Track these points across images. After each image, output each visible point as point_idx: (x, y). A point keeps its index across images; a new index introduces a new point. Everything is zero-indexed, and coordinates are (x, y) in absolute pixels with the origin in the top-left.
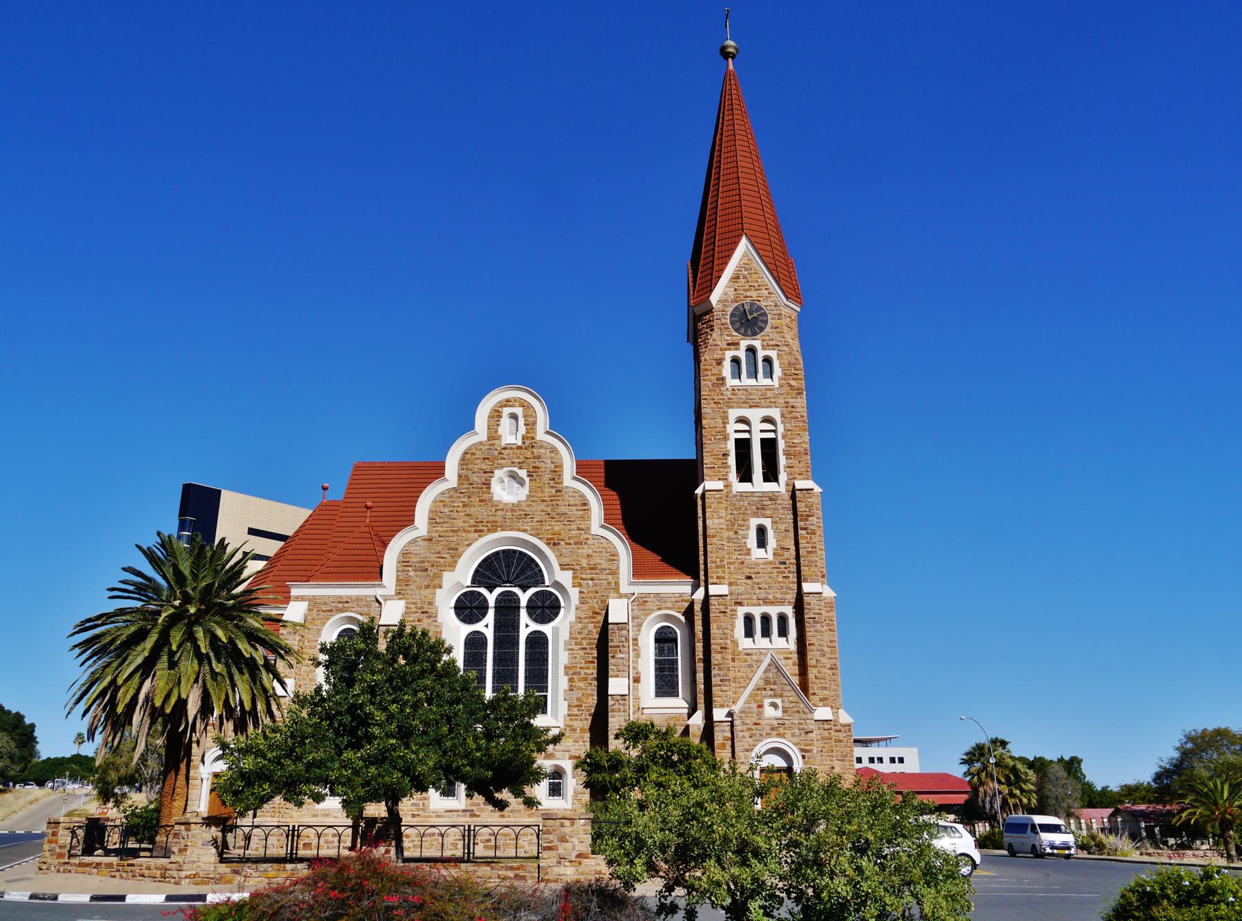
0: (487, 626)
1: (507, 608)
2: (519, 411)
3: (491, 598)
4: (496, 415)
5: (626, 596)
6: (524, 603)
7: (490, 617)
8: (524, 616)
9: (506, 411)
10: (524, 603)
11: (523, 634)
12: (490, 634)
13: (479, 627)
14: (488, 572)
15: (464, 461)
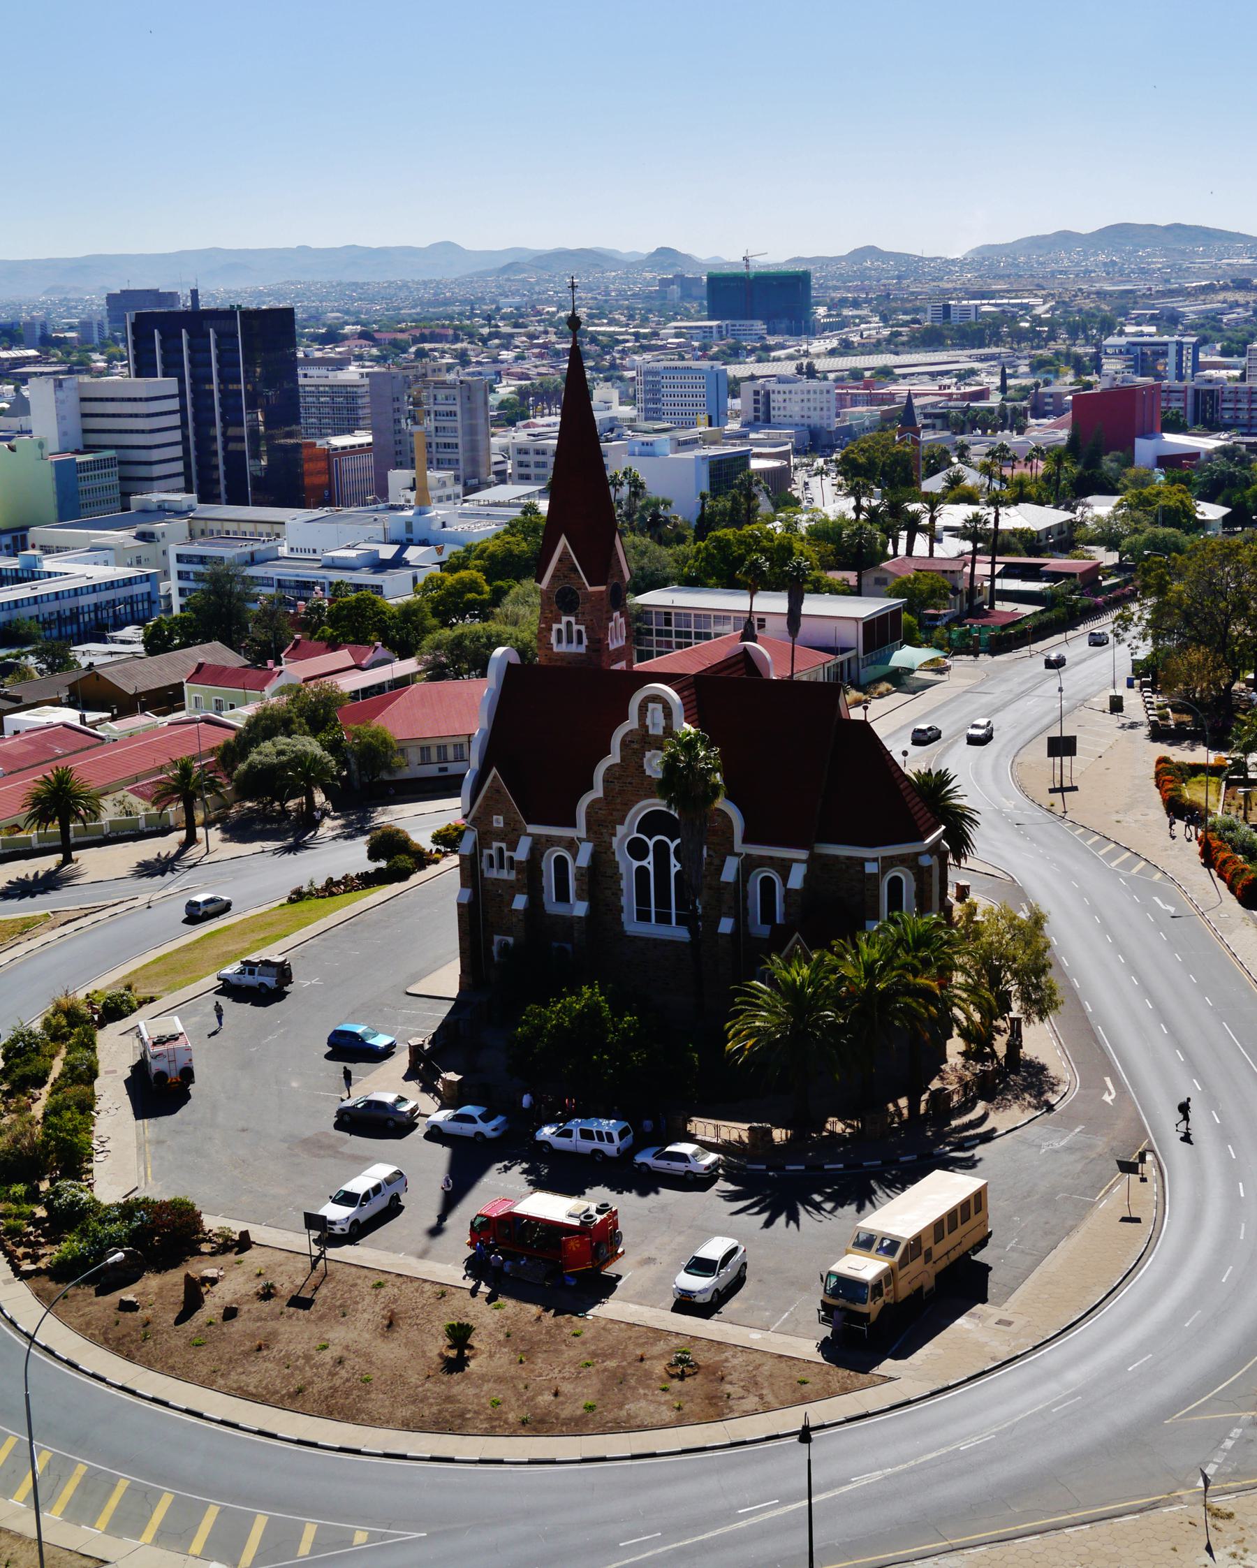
0: (649, 862)
1: (661, 849)
2: (659, 707)
3: (651, 844)
4: (643, 709)
5: (739, 855)
6: (672, 850)
7: (651, 857)
8: (673, 860)
9: (651, 706)
10: (672, 850)
11: (673, 871)
12: (651, 868)
13: (644, 863)
14: (651, 823)
15: (624, 744)
